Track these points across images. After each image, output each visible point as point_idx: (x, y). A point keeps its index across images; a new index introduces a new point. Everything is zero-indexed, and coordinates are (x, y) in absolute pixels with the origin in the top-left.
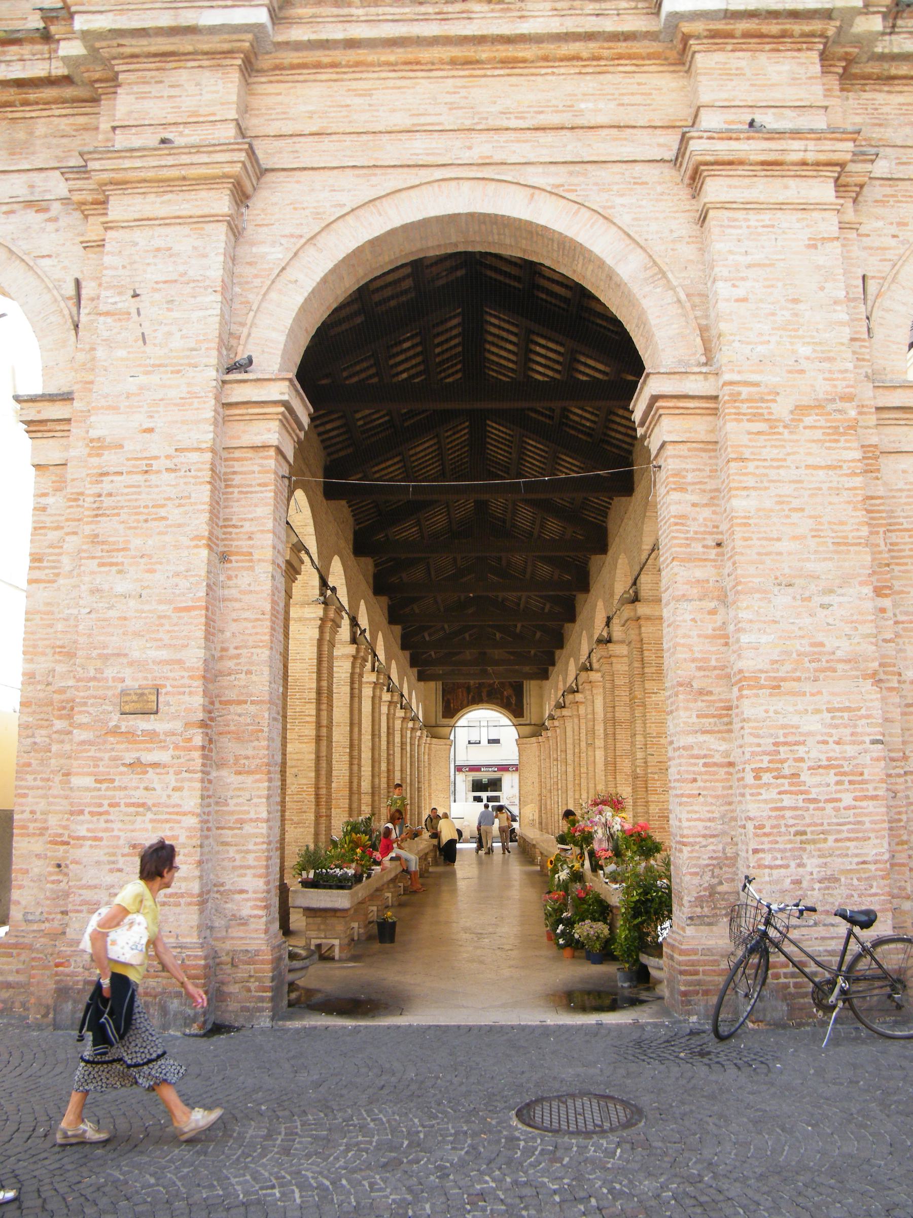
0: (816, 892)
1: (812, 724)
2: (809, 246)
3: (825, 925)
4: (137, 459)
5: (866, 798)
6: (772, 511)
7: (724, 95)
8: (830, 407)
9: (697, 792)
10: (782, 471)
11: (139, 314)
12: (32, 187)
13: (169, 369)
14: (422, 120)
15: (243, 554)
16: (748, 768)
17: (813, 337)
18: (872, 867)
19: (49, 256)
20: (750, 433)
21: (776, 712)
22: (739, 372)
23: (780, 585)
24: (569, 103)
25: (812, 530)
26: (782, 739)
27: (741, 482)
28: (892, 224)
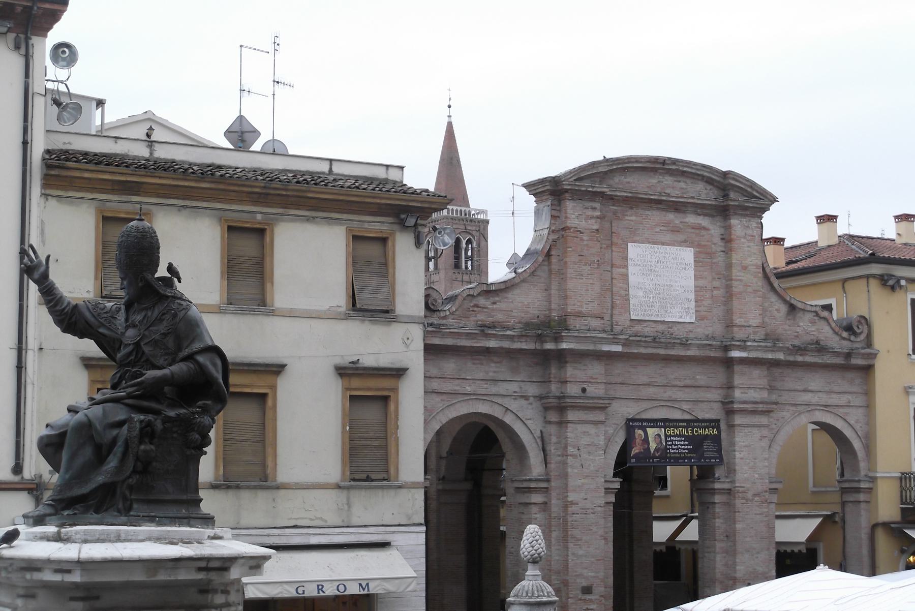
4: (583, 509)
8: (762, 494)
12: (521, 388)
14: (653, 380)
19: (530, 419)
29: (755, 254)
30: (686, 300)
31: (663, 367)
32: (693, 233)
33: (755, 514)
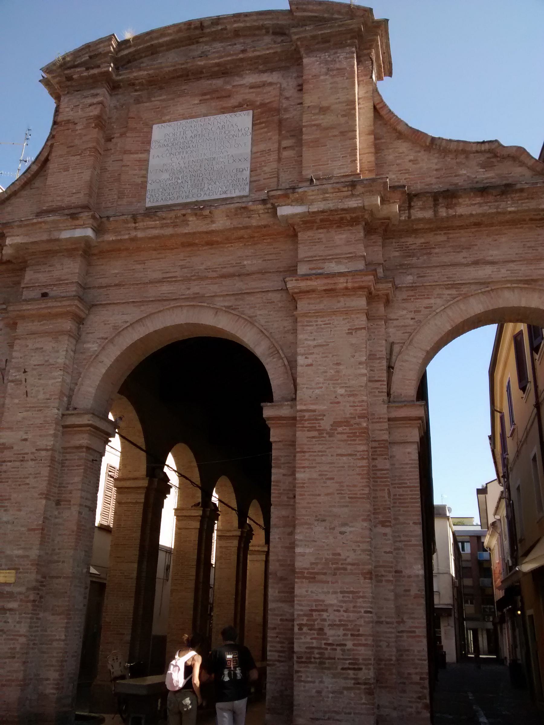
0: (330, 699)
1: (332, 600)
2: (348, 333)
3: (334, 720)
4: (19, 454)
5: (360, 645)
6: (316, 479)
7: (310, 254)
8: (353, 422)
9: (275, 635)
10: (323, 458)
11: (26, 382)
13: (37, 409)
15: (66, 501)
16: (296, 623)
17: (346, 383)
18: (363, 687)
20: (308, 438)
21: (312, 592)
22: (305, 405)
23: (318, 520)
24: (239, 262)
25: (337, 490)
26: (314, 608)
27: (301, 464)
28: (411, 312)
29: (343, 88)
30: (235, 171)
31: (189, 256)
32: (253, 92)
33: (338, 455)
